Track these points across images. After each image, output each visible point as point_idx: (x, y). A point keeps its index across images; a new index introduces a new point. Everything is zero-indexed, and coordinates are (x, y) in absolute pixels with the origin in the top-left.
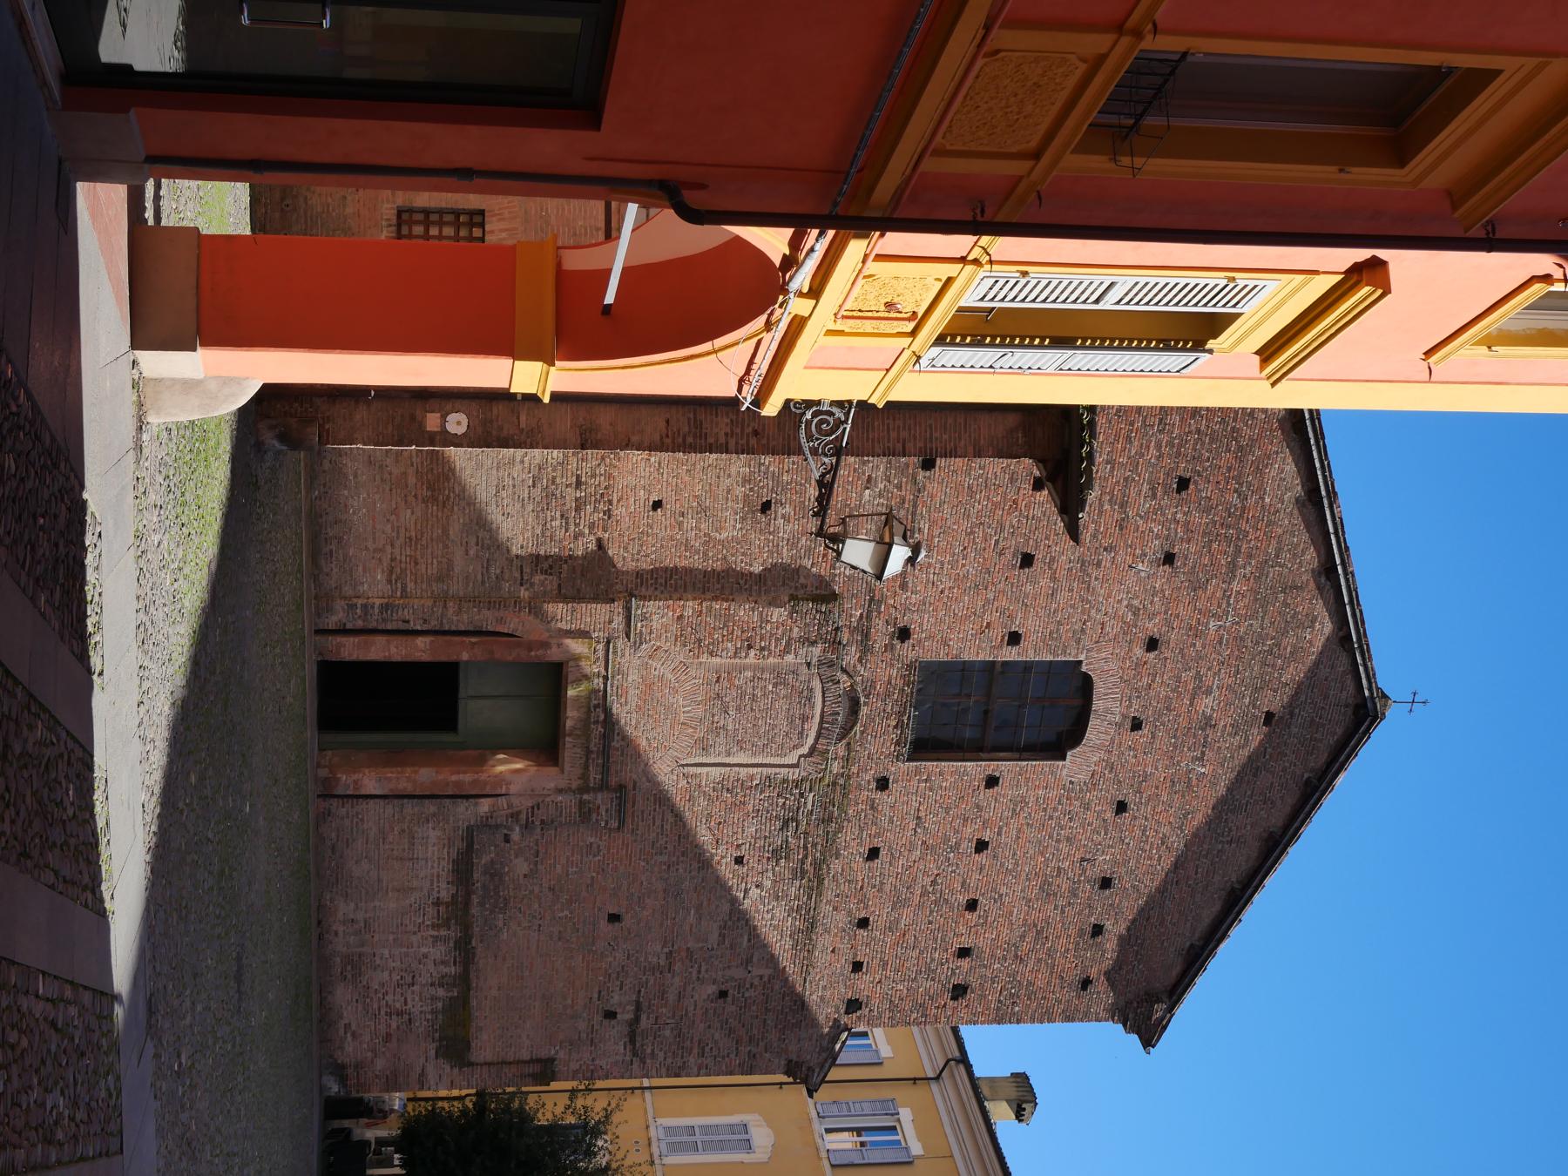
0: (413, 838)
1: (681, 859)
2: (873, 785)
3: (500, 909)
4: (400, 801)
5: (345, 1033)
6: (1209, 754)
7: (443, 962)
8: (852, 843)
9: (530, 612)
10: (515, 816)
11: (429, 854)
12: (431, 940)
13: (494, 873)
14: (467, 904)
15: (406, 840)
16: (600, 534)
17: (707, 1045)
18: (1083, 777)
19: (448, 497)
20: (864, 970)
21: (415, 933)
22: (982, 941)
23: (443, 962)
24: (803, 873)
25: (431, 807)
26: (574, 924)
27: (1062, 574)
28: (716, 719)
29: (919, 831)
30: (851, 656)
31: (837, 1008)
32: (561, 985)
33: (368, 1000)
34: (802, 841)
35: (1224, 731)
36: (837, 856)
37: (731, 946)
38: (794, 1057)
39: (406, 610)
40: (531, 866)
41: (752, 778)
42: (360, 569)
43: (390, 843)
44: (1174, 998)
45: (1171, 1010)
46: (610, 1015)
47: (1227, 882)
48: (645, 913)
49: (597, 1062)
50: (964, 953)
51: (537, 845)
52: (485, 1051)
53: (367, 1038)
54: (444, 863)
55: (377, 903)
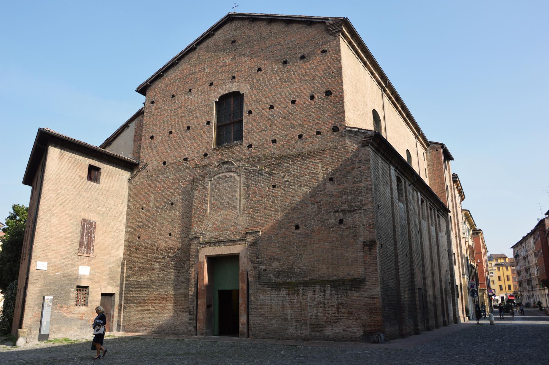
0: (263, 304)
3: (293, 270)
4: (250, 309)
5: (348, 331)
7: (314, 291)
8: (273, 149)
10: (255, 268)
11: (269, 298)
12: (304, 297)
13: (278, 274)
14: (289, 284)
15: (264, 307)
17: (355, 180)
18: (248, 86)
20: (320, 130)
21: (301, 303)
22: (307, 94)
23: (314, 291)
24: (279, 163)
26: (299, 242)
27: (192, 118)
28: (225, 205)
29: (266, 129)
30: (210, 169)
31: (336, 136)
32: (327, 243)
33: (332, 321)
36: (274, 153)
41: (244, 189)
43: (265, 312)
44: (324, 21)
45: (327, 19)
46: (341, 222)
47: (285, 26)
48: (295, 216)
49: (365, 224)
50: (312, 98)
51: (267, 259)
52: (360, 271)
53: (350, 322)
55: (289, 318)
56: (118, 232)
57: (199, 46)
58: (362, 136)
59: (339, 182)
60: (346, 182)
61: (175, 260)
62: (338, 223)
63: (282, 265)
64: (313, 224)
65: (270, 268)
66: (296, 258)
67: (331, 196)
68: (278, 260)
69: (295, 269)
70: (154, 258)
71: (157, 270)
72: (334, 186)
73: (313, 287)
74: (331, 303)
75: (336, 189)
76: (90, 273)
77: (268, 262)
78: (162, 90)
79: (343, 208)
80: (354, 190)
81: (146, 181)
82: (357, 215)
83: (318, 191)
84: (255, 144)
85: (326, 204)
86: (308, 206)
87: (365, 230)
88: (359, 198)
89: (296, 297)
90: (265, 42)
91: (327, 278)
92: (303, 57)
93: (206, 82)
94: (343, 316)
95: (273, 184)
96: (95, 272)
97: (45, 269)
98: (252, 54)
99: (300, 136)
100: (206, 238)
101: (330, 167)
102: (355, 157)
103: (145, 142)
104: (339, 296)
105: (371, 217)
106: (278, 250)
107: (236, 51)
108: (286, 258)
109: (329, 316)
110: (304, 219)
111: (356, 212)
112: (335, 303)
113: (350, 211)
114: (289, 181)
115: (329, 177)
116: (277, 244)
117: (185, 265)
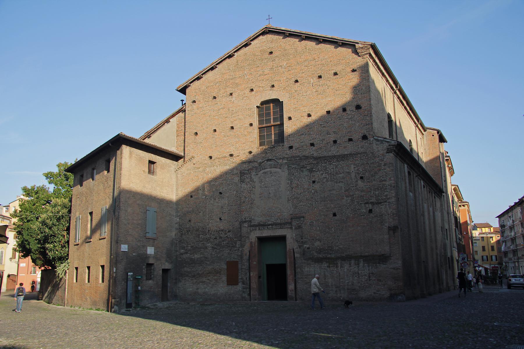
0: (308, 275)
1: (314, 198)
2: (291, 150)
5: (377, 294)
6: (281, 64)
7: (350, 264)
9: (244, 247)
10: (300, 247)
11: (313, 270)
12: (342, 269)
14: (329, 258)
16: (227, 232)
19: (219, 269)
21: (340, 273)
23: (350, 264)
25: (298, 270)
31: (365, 143)
32: (359, 228)
34: (307, 166)
35: (274, 63)
37: (343, 179)
38: (385, 151)
39: (244, 278)
40: (317, 240)
42: (236, 290)
48: (332, 206)
49: (390, 213)
51: (310, 240)
52: (386, 249)
54: (316, 266)
55: (330, 285)
56: (170, 216)
57: (237, 53)
58: (387, 144)
59: (368, 180)
60: (374, 180)
61: (226, 240)
62: (368, 212)
63: (323, 244)
64: (348, 213)
65: (312, 247)
66: (334, 238)
67: (362, 191)
68: (320, 240)
69: (333, 247)
70: (207, 239)
71: (210, 249)
72: (364, 183)
73: (349, 261)
74: (364, 273)
75: (366, 186)
76: (154, 253)
77: (311, 242)
78: (203, 91)
79: (372, 200)
80: (381, 187)
81: (193, 173)
82: (383, 206)
83: (351, 187)
84: (296, 145)
85: (358, 197)
86: (344, 199)
87: (390, 218)
88: (385, 193)
89: (336, 269)
90: (300, 56)
91: (360, 254)
92: (335, 74)
93: (246, 88)
94: (374, 283)
95: (313, 180)
96: (157, 252)
97: (127, 250)
98: (289, 66)
99: (335, 142)
100: (255, 222)
101: (361, 168)
102: (381, 161)
103: (190, 138)
104: (370, 268)
105: (394, 208)
106: (319, 233)
107: (273, 62)
108: (326, 238)
109: (363, 283)
110: (340, 208)
111: (382, 204)
112: (367, 273)
113: (377, 203)
114: (326, 178)
115: (360, 176)
116: (318, 228)
117: (236, 244)
